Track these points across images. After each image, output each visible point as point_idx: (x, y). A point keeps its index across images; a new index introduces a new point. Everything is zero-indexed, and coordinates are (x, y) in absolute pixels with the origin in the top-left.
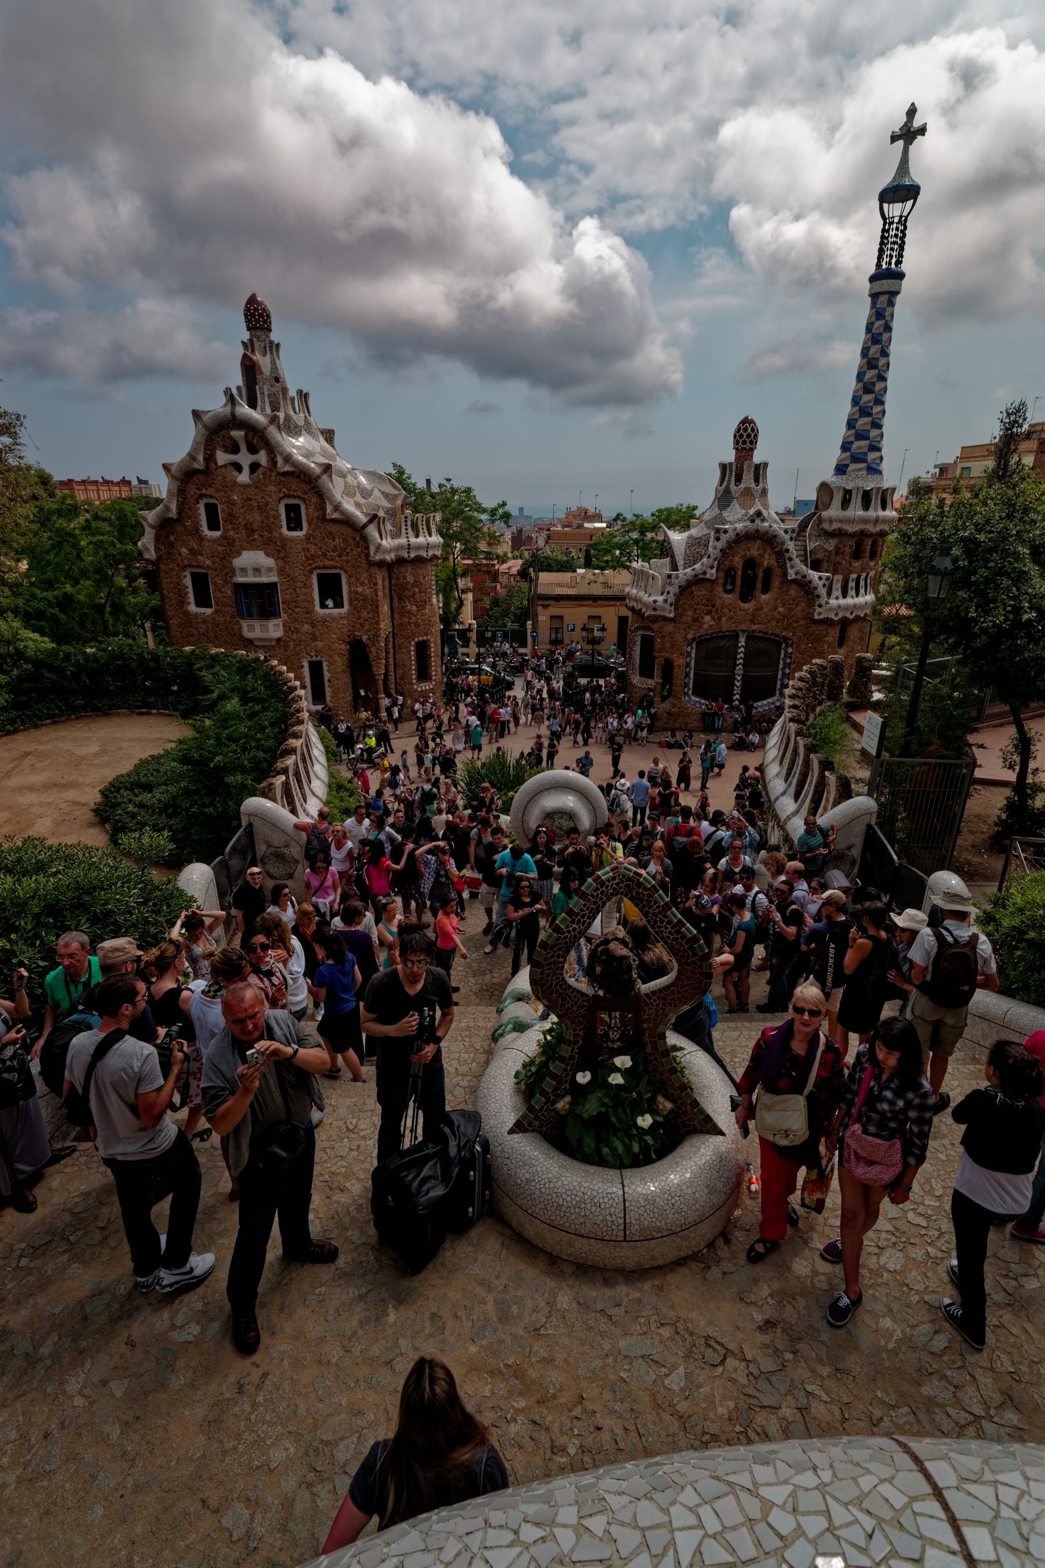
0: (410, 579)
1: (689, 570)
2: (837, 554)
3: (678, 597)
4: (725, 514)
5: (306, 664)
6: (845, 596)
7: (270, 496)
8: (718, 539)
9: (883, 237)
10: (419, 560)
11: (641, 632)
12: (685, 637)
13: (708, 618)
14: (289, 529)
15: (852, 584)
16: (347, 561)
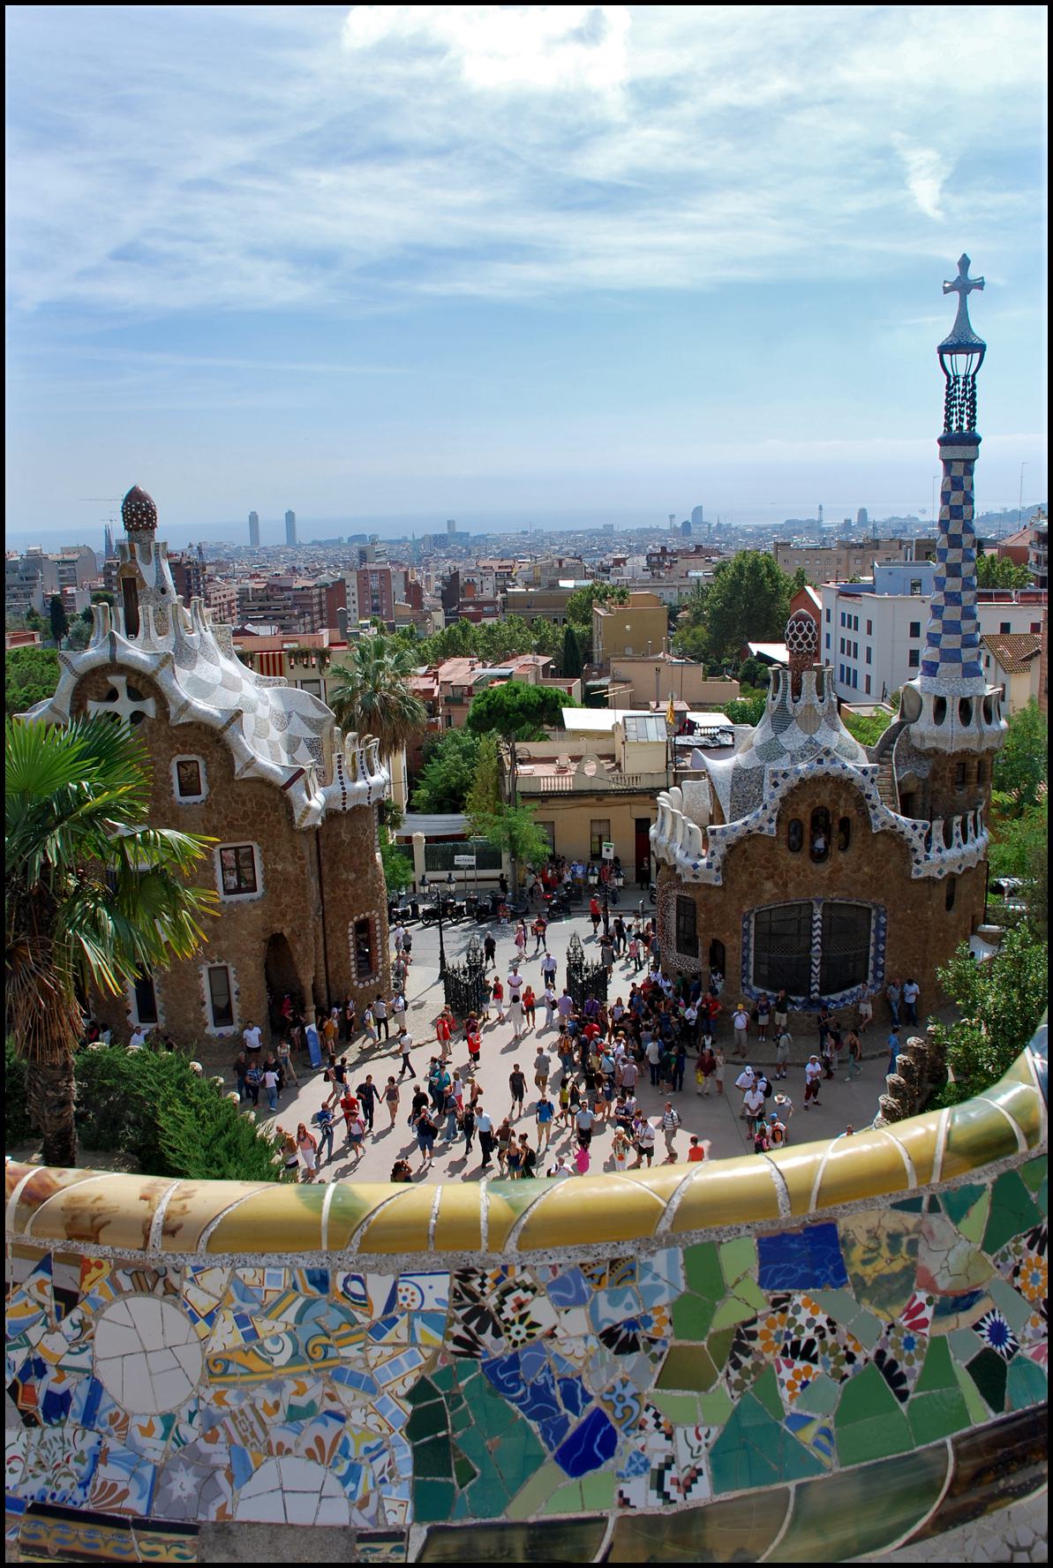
0: (346, 837)
1: (738, 823)
2: (934, 779)
3: (725, 859)
4: (783, 739)
5: (204, 972)
6: (948, 846)
7: (158, 754)
8: (776, 785)
9: (948, 395)
10: (358, 809)
11: (676, 892)
12: (739, 910)
13: (769, 885)
14: (184, 791)
15: (957, 829)
16: (262, 831)
